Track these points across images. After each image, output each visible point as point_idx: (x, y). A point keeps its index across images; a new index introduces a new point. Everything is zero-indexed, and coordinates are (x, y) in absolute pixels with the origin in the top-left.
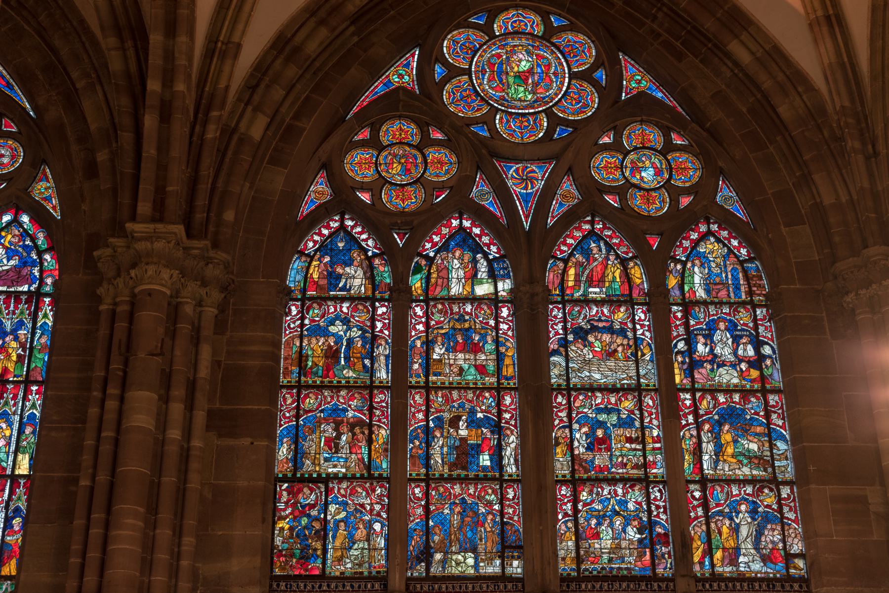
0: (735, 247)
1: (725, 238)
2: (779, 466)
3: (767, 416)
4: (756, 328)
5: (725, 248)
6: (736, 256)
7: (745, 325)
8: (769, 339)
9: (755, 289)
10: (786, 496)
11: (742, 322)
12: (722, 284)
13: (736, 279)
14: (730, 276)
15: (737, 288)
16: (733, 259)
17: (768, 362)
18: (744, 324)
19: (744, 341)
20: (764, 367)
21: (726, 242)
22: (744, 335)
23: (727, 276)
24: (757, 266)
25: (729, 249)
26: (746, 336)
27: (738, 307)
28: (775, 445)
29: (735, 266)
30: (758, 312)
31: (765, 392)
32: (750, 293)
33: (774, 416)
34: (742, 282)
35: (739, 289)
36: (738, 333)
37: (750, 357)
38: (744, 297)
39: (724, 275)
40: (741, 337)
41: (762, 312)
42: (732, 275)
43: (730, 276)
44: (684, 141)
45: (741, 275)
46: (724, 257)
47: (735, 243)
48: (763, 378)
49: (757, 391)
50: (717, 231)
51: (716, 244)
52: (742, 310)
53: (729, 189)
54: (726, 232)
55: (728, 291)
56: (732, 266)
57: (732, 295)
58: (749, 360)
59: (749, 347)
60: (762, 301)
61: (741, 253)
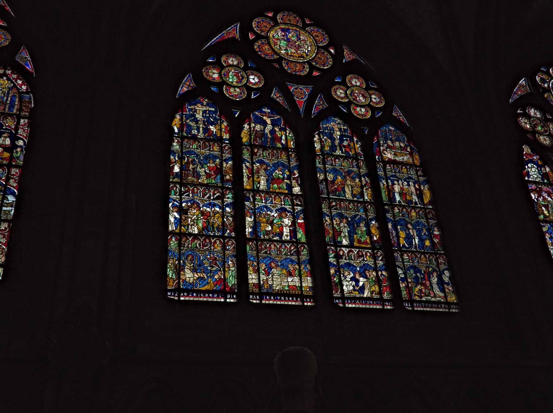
0: (18, 84)
1: (14, 79)
2: (5, 210)
3: (7, 180)
4: (17, 129)
5: (12, 84)
6: (18, 89)
7: (10, 127)
8: (24, 137)
9: (24, 108)
10: (3, 229)
11: (7, 124)
12: (3, 103)
13: (13, 101)
14: (9, 99)
15: (12, 106)
16: (15, 91)
17: (19, 149)
18: (8, 126)
19: (5, 135)
20: (15, 152)
21: (14, 81)
22: (6, 132)
23: (7, 100)
24: (31, 97)
25: (14, 84)
26: (8, 133)
27: (7, 116)
28: (7, 198)
29: (15, 94)
30: (22, 121)
31: (10, 166)
32: (20, 110)
33: (12, 181)
34: (16, 103)
35: (13, 107)
36: (2, 130)
37: (7, 145)
38: (15, 111)
39: (5, 98)
40: (4, 133)
41: (24, 121)
42: (11, 99)
43: (9, 99)
44: (4, 24)
45: (17, 99)
46: (9, 88)
47: (20, 82)
48: (11, 158)
49: (5, 165)
50: (9, 74)
51: (6, 81)
52: (9, 118)
53: (26, 53)
54: (16, 76)
55: (5, 107)
56: (13, 94)
57: (7, 109)
58: (5, 147)
59: (8, 139)
60: (26, 115)
61: (22, 88)
